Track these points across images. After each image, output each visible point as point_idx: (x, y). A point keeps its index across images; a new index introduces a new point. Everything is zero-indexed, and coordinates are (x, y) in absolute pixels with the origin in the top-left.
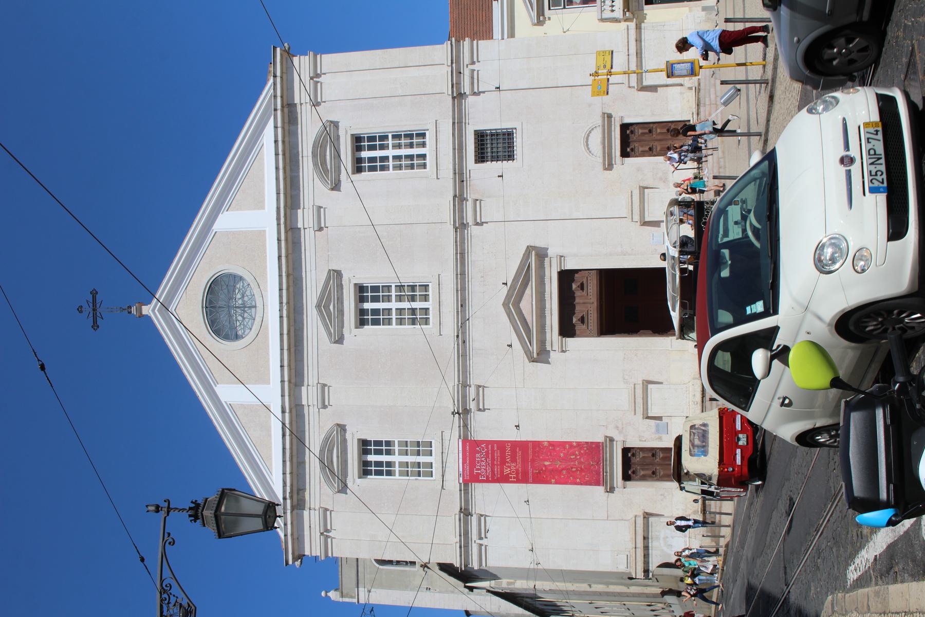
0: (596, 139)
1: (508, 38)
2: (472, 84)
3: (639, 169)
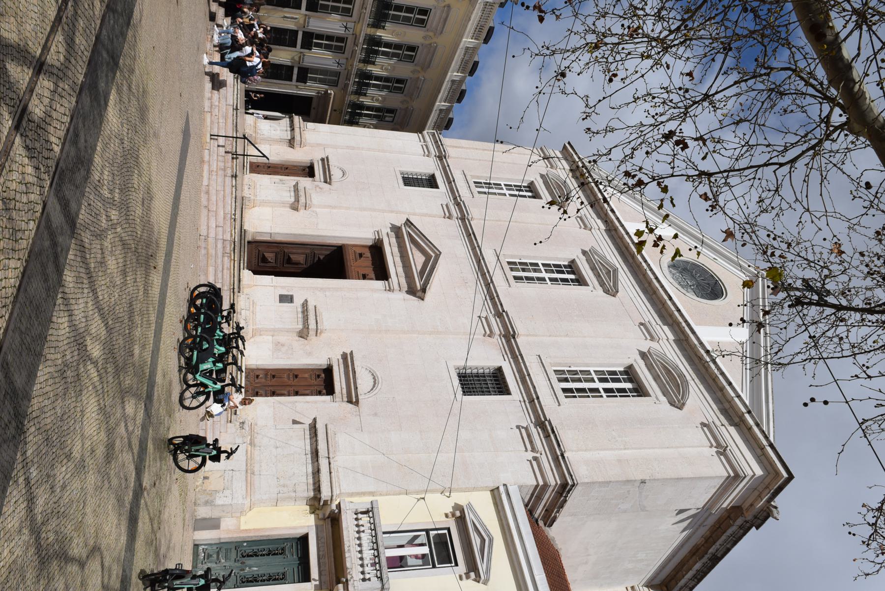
0: (364, 382)
1: (498, 488)
2: (529, 436)
3: (310, 354)
